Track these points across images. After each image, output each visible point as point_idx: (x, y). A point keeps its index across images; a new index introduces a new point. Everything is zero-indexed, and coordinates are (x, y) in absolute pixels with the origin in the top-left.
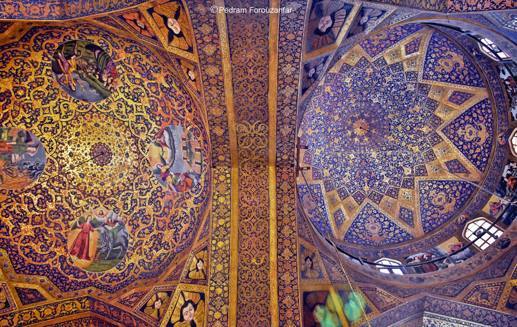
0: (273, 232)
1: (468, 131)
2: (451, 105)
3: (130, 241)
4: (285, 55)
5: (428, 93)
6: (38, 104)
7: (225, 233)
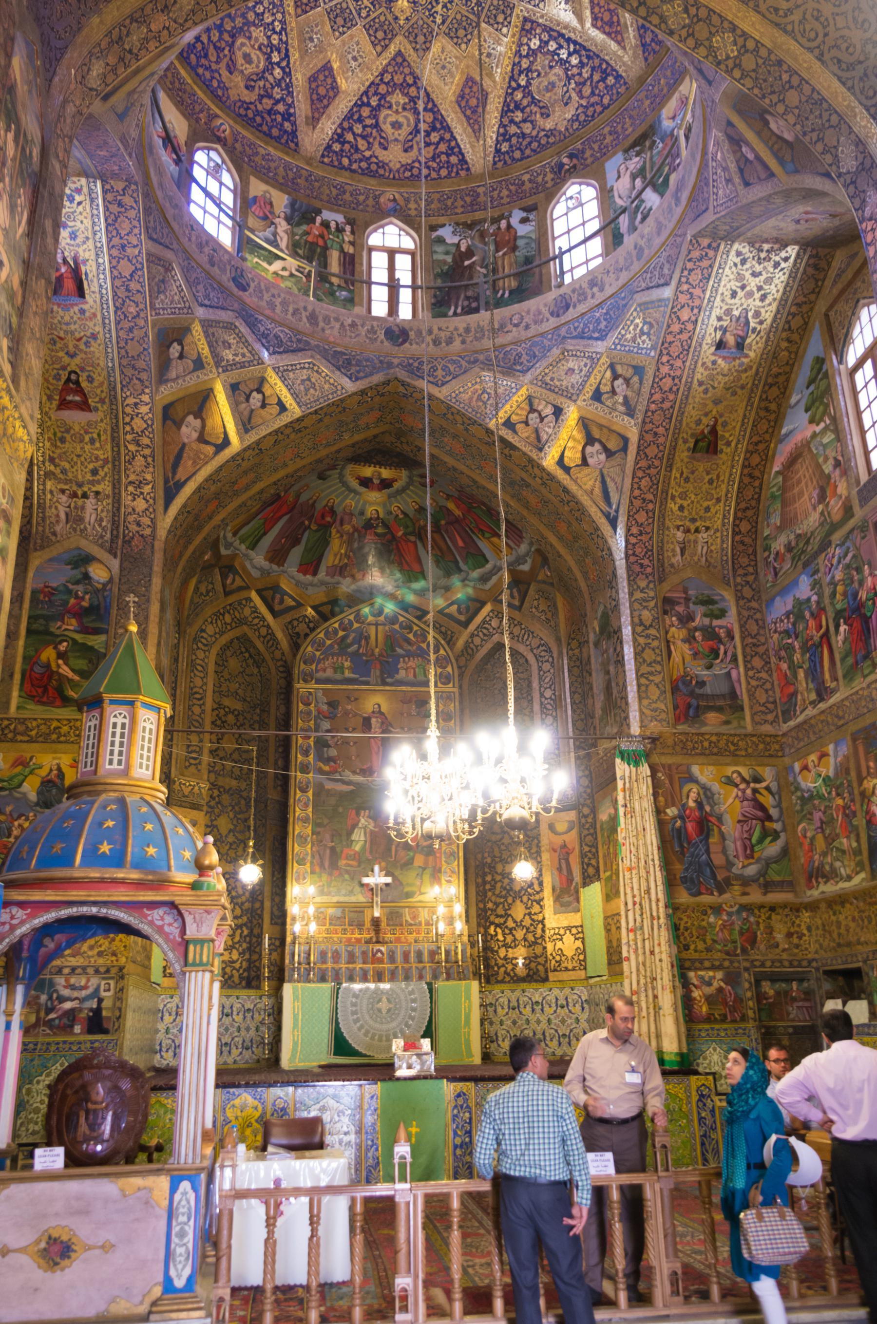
1: (401, 120)
2: (458, 79)
4: (760, 61)
5: (488, 23)
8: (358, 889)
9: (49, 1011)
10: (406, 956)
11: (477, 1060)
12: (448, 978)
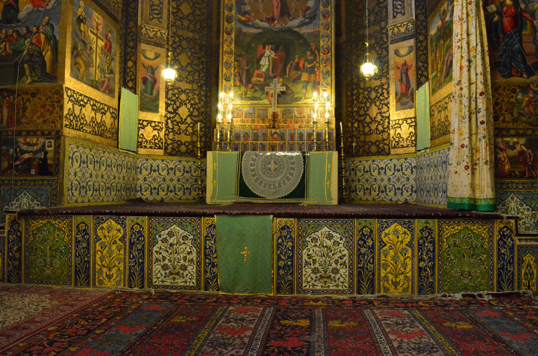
8: (264, 96)
9: (17, 159)
10: (292, 137)
11: (335, 202)
12: (319, 149)
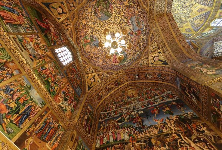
0: (172, 31)
3: (127, 54)
6: (93, 26)
7: (159, 36)
